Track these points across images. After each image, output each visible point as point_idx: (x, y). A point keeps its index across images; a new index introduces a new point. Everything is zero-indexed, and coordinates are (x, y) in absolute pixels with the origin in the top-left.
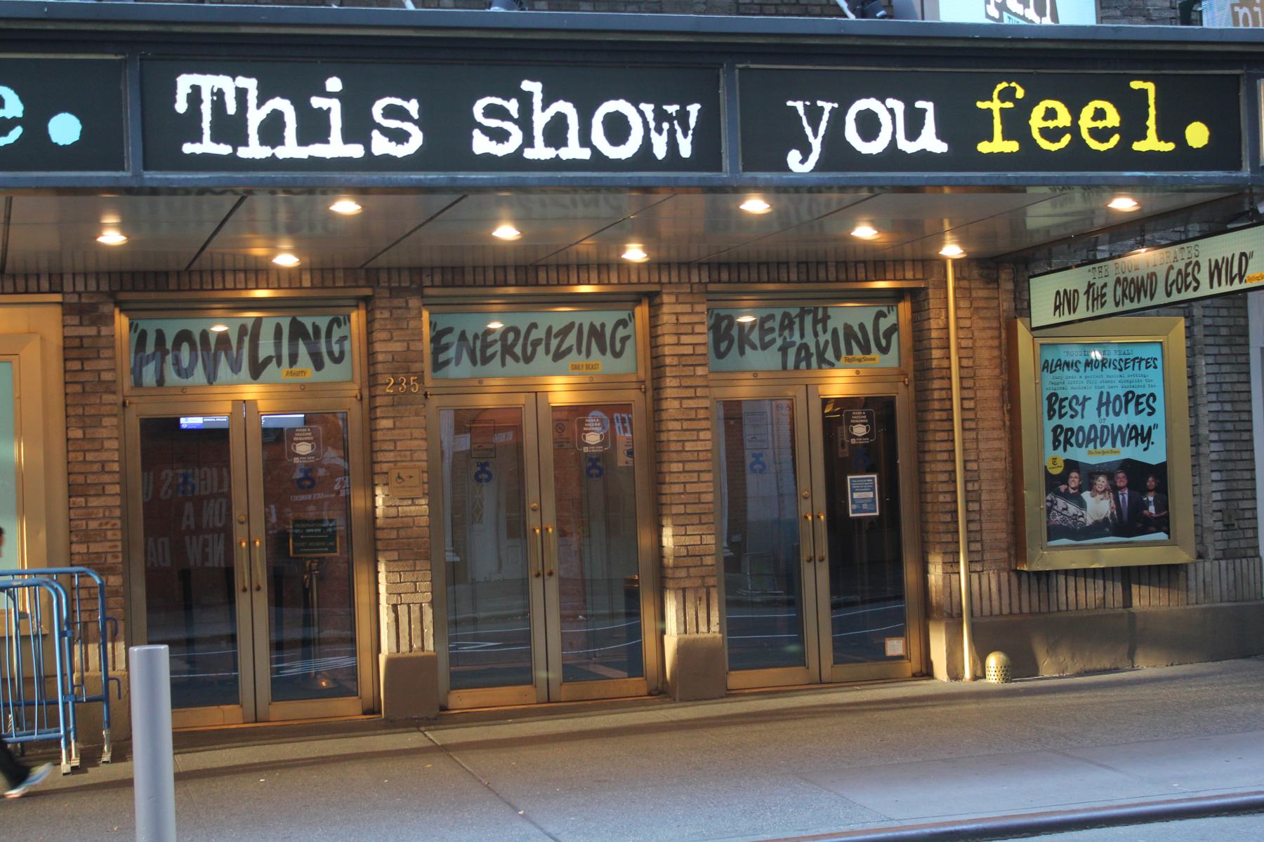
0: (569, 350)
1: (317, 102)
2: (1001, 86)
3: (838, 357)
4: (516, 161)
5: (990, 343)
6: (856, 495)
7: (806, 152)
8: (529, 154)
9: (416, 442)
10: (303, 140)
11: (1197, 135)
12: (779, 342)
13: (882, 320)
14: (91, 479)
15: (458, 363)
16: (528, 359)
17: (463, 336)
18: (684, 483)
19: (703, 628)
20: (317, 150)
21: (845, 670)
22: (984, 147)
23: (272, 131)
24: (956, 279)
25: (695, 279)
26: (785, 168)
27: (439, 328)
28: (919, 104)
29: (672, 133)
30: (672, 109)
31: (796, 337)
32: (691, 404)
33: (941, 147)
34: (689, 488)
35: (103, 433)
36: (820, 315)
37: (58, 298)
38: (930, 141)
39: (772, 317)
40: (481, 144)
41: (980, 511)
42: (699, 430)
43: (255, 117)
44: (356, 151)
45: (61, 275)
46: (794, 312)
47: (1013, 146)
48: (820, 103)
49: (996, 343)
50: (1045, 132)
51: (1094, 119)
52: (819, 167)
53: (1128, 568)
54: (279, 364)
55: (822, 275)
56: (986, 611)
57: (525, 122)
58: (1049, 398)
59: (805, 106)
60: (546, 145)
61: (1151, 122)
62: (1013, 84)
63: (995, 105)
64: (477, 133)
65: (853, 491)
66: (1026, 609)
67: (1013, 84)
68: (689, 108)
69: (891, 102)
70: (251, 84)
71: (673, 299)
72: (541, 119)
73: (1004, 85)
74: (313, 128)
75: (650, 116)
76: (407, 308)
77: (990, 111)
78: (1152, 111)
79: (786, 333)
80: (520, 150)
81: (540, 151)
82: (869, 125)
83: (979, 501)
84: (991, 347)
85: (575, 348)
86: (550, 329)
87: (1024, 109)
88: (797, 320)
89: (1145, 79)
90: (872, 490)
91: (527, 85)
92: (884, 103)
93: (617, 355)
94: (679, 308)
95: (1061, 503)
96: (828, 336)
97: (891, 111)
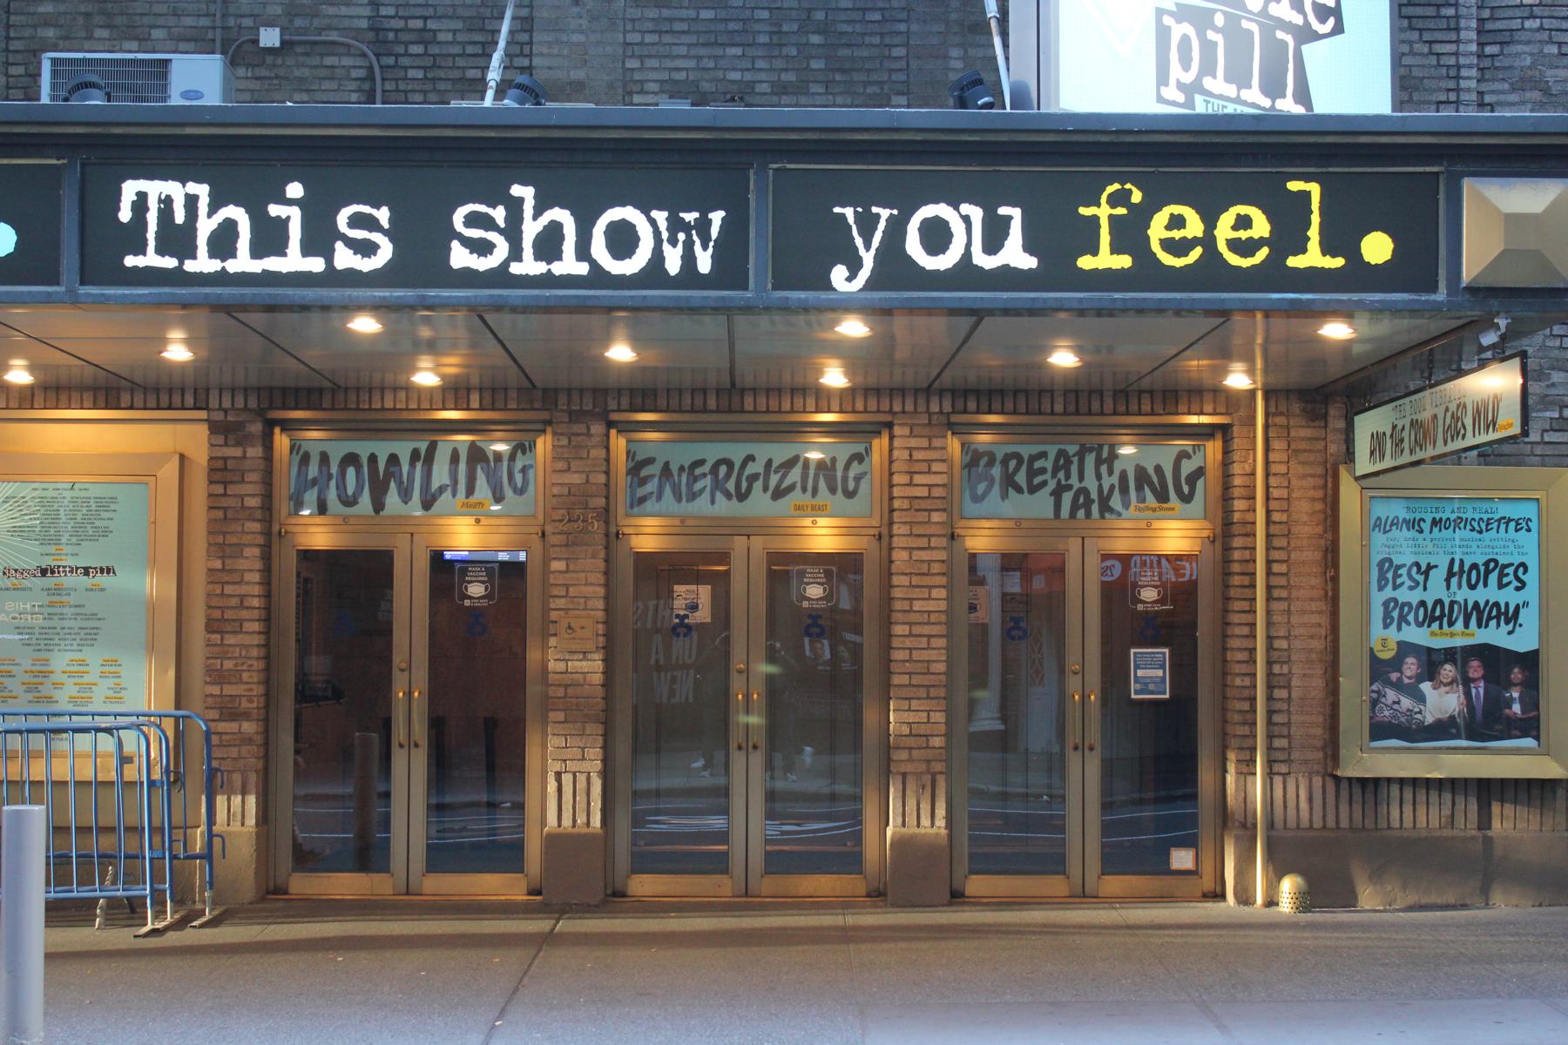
0: (791, 488)
1: (275, 210)
2: (1110, 189)
3: (1126, 505)
4: (500, 276)
5: (1311, 493)
6: (1140, 673)
7: (854, 266)
8: (516, 269)
9: (590, 589)
10: (257, 252)
11: (1377, 248)
12: (1052, 485)
13: (1185, 462)
14: (229, 614)
15: (659, 498)
16: (742, 497)
17: (666, 468)
19: (925, 822)
20: (273, 264)
21: (1115, 884)
22: (1086, 263)
23: (223, 242)
24: (1267, 414)
25: (935, 408)
26: (829, 287)
27: (639, 458)
29: (689, 245)
30: (690, 217)
31: (1074, 480)
32: (924, 555)
33: (1029, 262)
34: (916, 655)
35: (242, 564)
36: (1105, 454)
37: (203, 414)
38: (1015, 254)
39: (1044, 455)
40: (460, 257)
41: (1289, 699)
42: (931, 587)
43: (206, 227)
44: (316, 265)
45: (208, 390)
46: (1072, 449)
48: (875, 210)
49: (1320, 494)
50: (1167, 245)
52: (870, 285)
54: (454, 495)
55: (1096, 406)
56: (1292, 823)
57: (513, 233)
58: (1381, 564)
59: (856, 212)
60: (536, 259)
61: (1314, 233)
63: (1103, 212)
64: (455, 244)
65: (1137, 667)
66: (1344, 823)
67: (1128, 186)
68: (711, 216)
69: (966, 208)
70: (202, 191)
71: (906, 431)
72: (531, 229)
73: (1117, 186)
74: (270, 239)
75: (663, 225)
76: (588, 434)
77: (1096, 218)
78: (1315, 219)
79: (1061, 475)
80: (505, 265)
81: (529, 266)
82: (936, 236)
83: (1288, 687)
84: (1313, 499)
85: (799, 485)
86: (769, 463)
87: (1141, 216)
88: (1075, 460)
89: (1307, 178)
90: (1162, 667)
91: (517, 190)
92: (957, 208)
93: (850, 495)
94: (913, 443)
95: (1391, 695)
96: (1115, 479)
97: (967, 220)
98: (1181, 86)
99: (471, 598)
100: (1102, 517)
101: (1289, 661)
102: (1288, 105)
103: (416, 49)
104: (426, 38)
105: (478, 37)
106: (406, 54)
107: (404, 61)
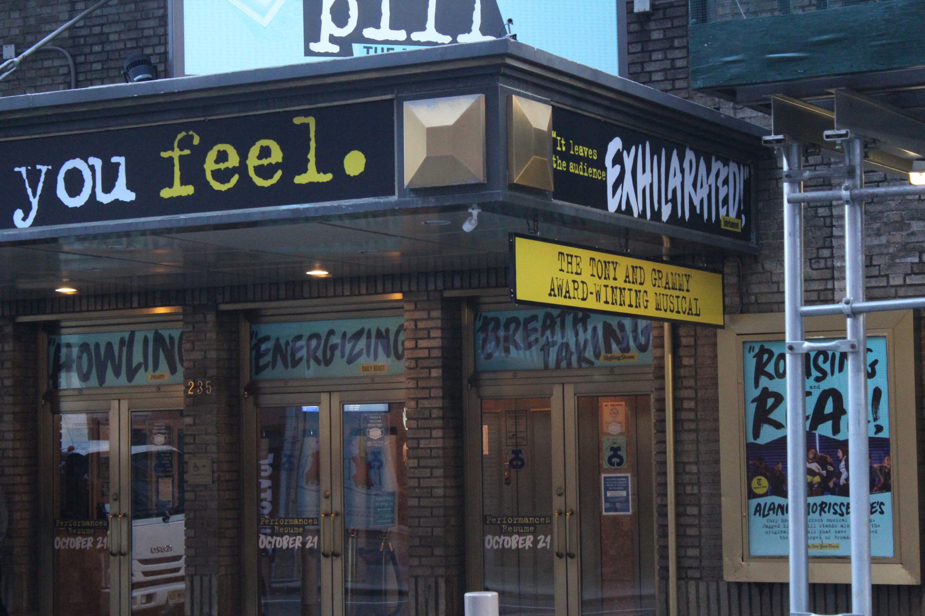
0: (360, 353)
2: (180, 136)
6: (609, 494)
7: (27, 211)
9: (208, 437)
11: (355, 163)
12: (543, 341)
15: (274, 367)
16: (328, 362)
18: (419, 478)
22: (166, 193)
25: (431, 287)
28: (115, 159)
32: (426, 404)
34: (423, 483)
38: (122, 193)
42: (431, 429)
47: (189, 190)
48: (38, 167)
51: (217, 162)
52: (35, 224)
53: (888, 587)
54: (146, 370)
59: (27, 170)
61: (312, 156)
62: (191, 133)
65: (606, 489)
67: (191, 133)
69: (93, 161)
73: (184, 134)
77: (171, 159)
78: (313, 144)
79: (548, 333)
82: (75, 183)
83: (699, 505)
85: (364, 351)
86: (344, 335)
87: (199, 155)
88: (558, 320)
89: (305, 113)
92: (86, 162)
97: (92, 168)
98: (333, 39)
99: (372, 440)
100: (580, 367)
101: (699, 484)
102: (474, 36)
103: (97, 48)
104: (103, 39)
105: (133, 35)
106: (91, 53)
107: (91, 58)
